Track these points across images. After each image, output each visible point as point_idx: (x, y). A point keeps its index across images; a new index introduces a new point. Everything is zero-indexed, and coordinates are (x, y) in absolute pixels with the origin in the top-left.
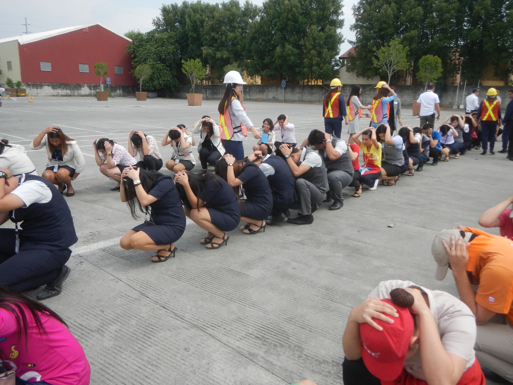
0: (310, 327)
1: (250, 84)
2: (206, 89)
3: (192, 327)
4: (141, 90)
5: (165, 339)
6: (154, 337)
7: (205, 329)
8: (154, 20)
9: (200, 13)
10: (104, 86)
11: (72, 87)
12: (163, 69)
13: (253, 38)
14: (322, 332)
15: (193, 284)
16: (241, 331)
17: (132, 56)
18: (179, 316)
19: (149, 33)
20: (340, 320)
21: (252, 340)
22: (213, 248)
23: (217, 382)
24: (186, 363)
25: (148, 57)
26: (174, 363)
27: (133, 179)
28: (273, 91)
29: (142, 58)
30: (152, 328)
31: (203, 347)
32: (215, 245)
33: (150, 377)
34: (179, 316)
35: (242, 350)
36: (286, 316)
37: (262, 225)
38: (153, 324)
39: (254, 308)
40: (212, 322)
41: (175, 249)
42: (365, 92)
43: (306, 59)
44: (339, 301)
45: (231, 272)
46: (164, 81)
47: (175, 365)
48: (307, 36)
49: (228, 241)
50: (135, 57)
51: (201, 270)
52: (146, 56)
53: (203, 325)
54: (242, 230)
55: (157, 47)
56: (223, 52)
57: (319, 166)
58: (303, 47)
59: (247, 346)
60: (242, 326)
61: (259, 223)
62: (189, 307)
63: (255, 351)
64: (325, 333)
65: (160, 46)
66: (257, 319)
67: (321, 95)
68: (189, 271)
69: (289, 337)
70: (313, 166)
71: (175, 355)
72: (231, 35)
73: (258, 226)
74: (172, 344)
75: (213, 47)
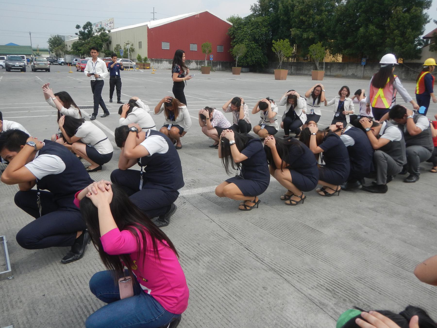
0: (380, 290)
2: (292, 65)
3: (270, 270)
4: (236, 65)
5: (247, 276)
6: (239, 272)
7: (282, 274)
8: (252, 7)
10: (208, 61)
13: (339, 21)
14: (392, 296)
15: (272, 233)
16: (313, 281)
17: (232, 37)
18: (260, 259)
19: (247, 18)
20: (411, 288)
21: (323, 291)
22: (291, 204)
23: (290, 322)
24: (264, 300)
26: (253, 297)
27: (229, 139)
28: (353, 68)
29: (240, 39)
30: (237, 265)
31: (279, 289)
32: (293, 202)
33: (233, 305)
34: (260, 259)
35: (313, 298)
36: (356, 275)
37: (337, 189)
38: (238, 262)
39: (325, 262)
40: (288, 269)
41: (259, 201)
43: (388, 39)
44: (411, 270)
45: (306, 227)
46: (256, 58)
47: (254, 299)
48: (392, 17)
49: (305, 200)
50: (234, 38)
51: (279, 222)
53: (280, 270)
54: (318, 192)
55: (253, 29)
56: (309, 33)
57: (399, 140)
58: (386, 28)
59: (318, 296)
60: (314, 277)
61: (335, 188)
62: (268, 253)
63: (326, 301)
64: (395, 298)
66: (328, 273)
67: (401, 72)
68: (270, 222)
69: (358, 295)
70: (392, 140)
71: (255, 291)
72: (318, 18)
73: (333, 190)
74: (253, 281)
75: (301, 28)
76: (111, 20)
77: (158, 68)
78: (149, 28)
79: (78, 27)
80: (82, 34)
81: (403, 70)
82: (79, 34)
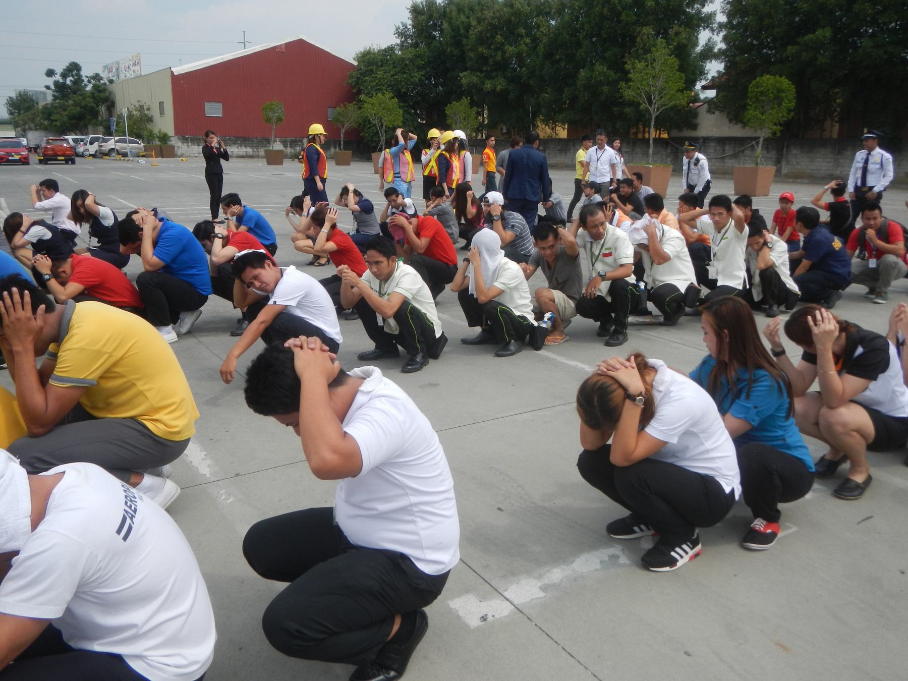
1: (546, 138)
9: (467, 12)
11: (255, 143)
13: (549, 56)
17: (355, 91)
42: (743, 151)
67: (664, 156)
75: (482, 72)
76: (135, 59)
77: (197, 155)
79: (50, 73)
80: (60, 88)
81: (669, 151)
82: (53, 87)
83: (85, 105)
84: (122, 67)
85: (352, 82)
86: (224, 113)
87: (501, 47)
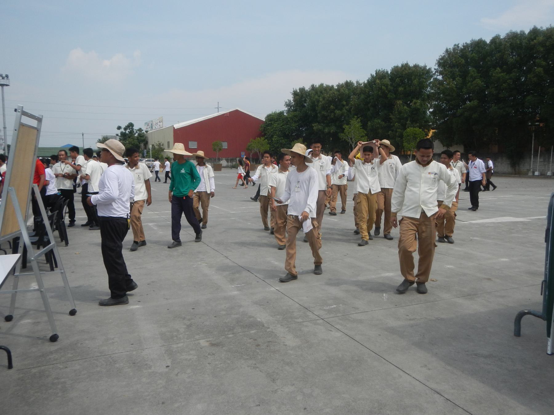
9: (319, 94)
12: (286, 144)
25: (274, 134)
29: (269, 135)
52: (273, 133)
55: (283, 125)
65: (285, 124)
78: (175, 128)
79: (119, 128)
82: (120, 135)
83: (134, 143)
84: (154, 123)
85: (262, 129)
86: (198, 147)
87: (333, 111)
